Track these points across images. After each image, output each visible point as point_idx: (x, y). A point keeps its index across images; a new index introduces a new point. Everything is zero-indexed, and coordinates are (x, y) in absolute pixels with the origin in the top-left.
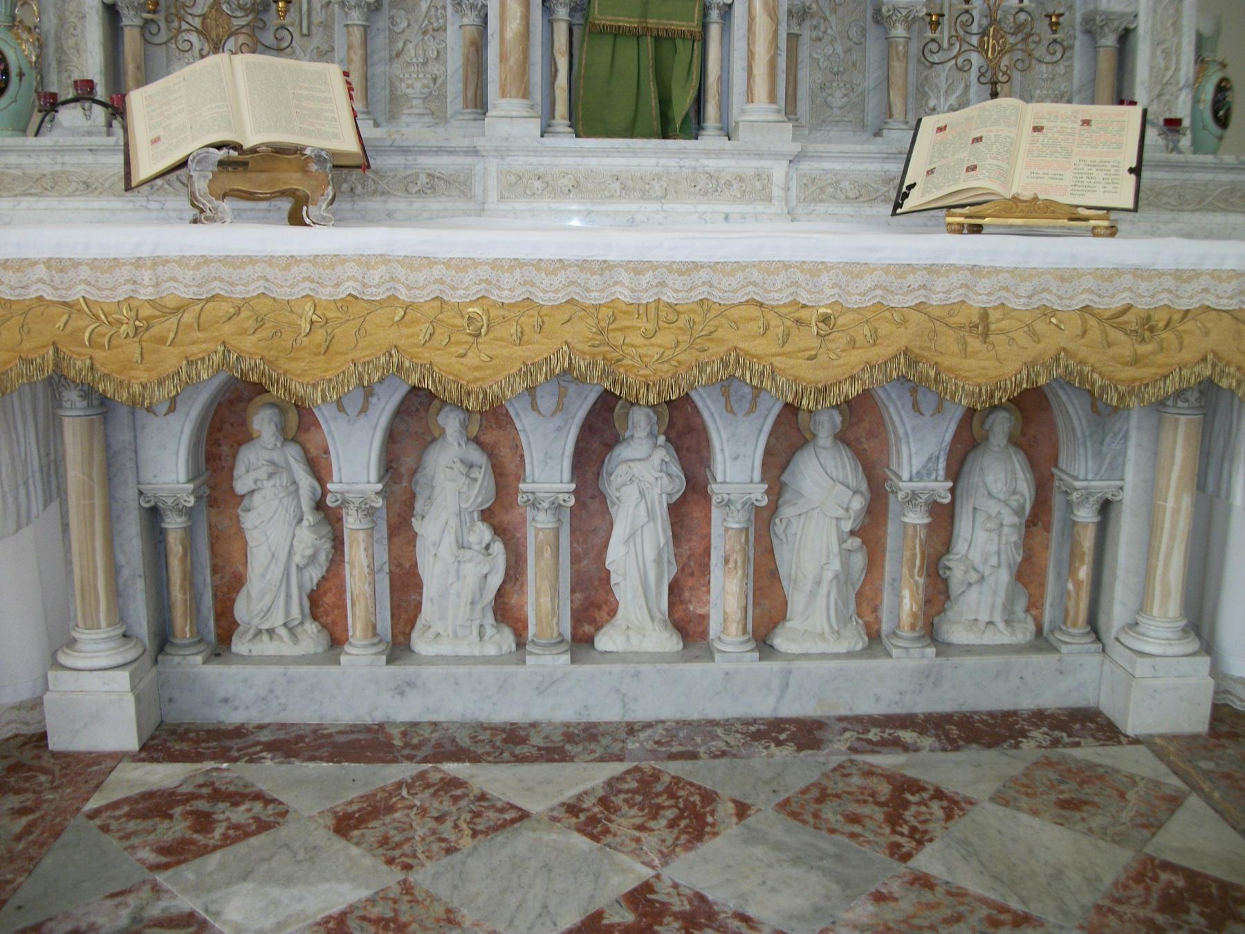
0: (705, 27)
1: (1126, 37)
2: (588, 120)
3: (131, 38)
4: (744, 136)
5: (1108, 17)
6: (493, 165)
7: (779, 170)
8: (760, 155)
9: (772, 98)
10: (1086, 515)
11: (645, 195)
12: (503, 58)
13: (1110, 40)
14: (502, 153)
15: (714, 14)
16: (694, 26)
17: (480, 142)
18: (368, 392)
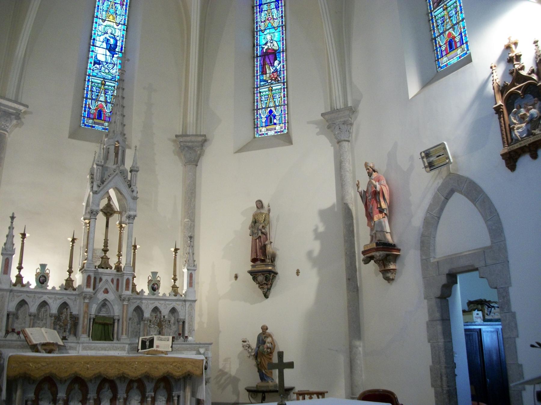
0: (114, 323)
1: (184, 322)
2: (96, 337)
3: (10, 320)
4: (122, 341)
5: (181, 319)
6: (81, 345)
7: (127, 346)
8: (124, 344)
9: (126, 334)
10: (176, 398)
11: (105, 350)
12: (83, 327)
13: (181, 323)
14: (83, 343)
15: (116, 321)
16: (112, 322)
17: (79, 341)
18: (66, 381)
